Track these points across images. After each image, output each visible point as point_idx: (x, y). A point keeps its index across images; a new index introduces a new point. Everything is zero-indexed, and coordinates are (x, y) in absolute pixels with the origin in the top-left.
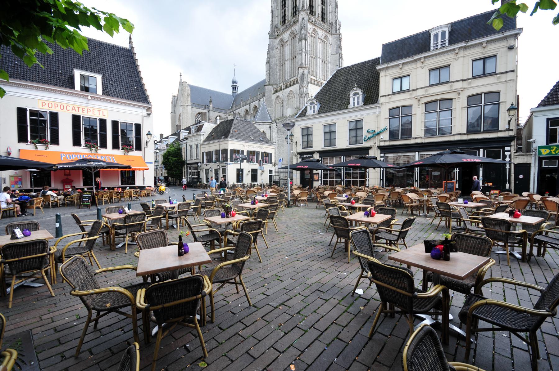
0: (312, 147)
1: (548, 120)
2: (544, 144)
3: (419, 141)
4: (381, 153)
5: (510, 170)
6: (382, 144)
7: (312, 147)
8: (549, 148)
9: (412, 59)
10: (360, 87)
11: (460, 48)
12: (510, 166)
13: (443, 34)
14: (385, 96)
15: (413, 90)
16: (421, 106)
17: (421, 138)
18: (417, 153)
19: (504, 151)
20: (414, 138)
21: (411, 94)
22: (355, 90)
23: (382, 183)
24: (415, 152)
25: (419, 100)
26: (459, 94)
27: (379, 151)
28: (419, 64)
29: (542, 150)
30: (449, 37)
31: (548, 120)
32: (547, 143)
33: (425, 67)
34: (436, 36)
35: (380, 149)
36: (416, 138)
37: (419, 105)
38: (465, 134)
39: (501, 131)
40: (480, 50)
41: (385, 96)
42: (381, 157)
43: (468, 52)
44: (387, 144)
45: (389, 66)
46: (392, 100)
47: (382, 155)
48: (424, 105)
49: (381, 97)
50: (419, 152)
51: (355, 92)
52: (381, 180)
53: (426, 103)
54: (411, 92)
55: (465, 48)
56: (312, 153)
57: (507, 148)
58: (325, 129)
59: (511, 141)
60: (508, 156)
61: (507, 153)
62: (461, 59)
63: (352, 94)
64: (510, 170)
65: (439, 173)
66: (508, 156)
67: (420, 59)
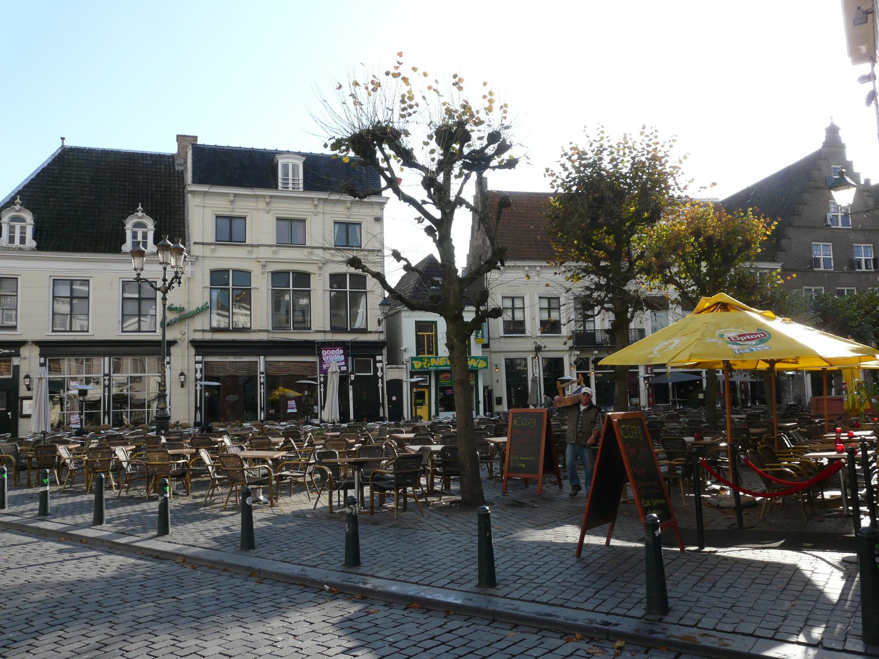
0: (14, 328)
1: (417, 322)
2: (414, 355)
3: (264, 337)
4: (196, 355)
5: (383, 388)
6: (199, 336)
7: (14, 328)
8: (421, 360)
9: (253, 193)
10: (148, 212)
11: (319, 199)
12: (382, 383)
13: (295, 167)
14: (203, 244)
15: (252, 246)
16: (265, 276)
17: (268, 331)
18: (262, 358)
19: (375, 362)
20: (255, 331)
21: (250, 252)
22: (141, 218)
23: (198, 415)
24: (260, 355)
25: (264, 266)
26: (320, 268)
27: (193, 351)
28: (262, 205)
29: (415, 362)
30: (304, 177)
31: (417, 322)
32: (417, 354)
33: (271, 212)
34: (286, 166)
35: (195, 347)
36: (260, 331)
37: (263, 273)
38: (328, 332)
39: (370, 332)
40: (342, 209)
41: (203, 244)
42: (197, 362)
43: (328, 208)
44: (208, 336)
45: (211, 190)
46: (216, 255)
47: (199, 358)
48: (270, 274)
49: (195, 243)
50: (265, 356)
51: (137, 220)
52: (196, 409)
53: (274, 274)
54: (250, 248)
55: (325, 201)
56: (17, 346)
57: (378, 358)
58: (57, 288)
59: (383, 347)
60: (380, 369)
61: (379, 365)
62: (321, 216)
63: (129, 224)
64: (383, 388)
65: (227, 398)
66: (380, 369)
67: (264, 196)
